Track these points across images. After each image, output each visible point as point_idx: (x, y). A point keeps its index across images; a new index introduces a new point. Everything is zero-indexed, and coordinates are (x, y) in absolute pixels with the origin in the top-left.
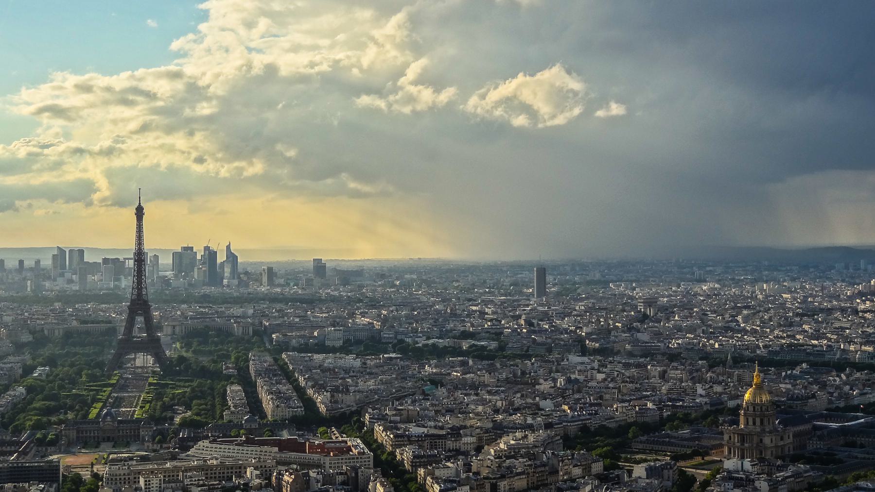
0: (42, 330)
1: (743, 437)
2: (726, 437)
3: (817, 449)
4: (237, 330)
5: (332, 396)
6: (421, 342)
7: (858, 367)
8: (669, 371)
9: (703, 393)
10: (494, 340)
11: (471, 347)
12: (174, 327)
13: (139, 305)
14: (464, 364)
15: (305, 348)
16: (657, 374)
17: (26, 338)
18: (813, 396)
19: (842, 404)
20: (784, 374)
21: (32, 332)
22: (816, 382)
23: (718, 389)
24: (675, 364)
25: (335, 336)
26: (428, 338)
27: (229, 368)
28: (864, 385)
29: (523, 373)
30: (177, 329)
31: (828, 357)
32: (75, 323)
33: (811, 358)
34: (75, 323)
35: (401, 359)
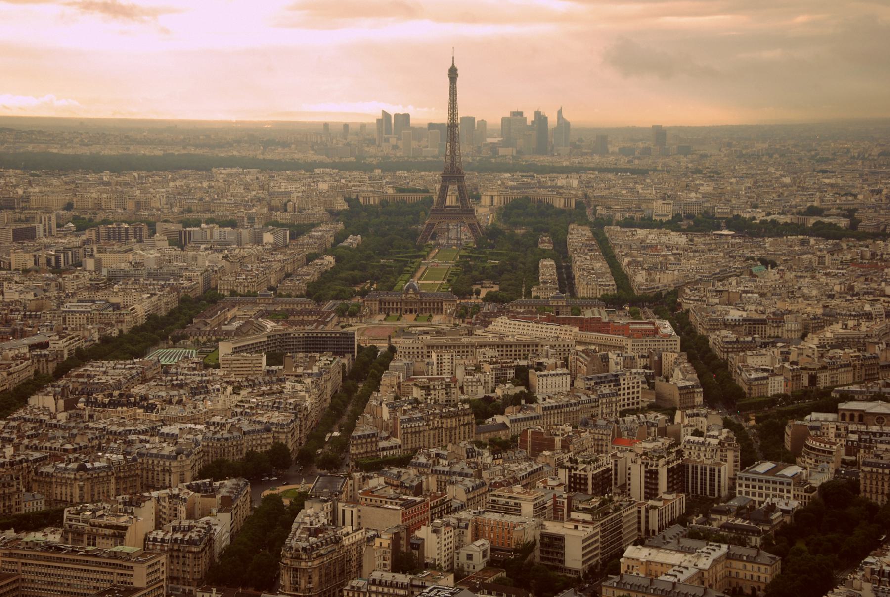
0: (357, 198)
4: (559, 203)
5: (650, 274)
6: (760, 216)
10: (844, 216)
11: (815, 224)
12: (492, 197)
13: (452, 174)
14: (803, 243)
15: (629, 224)
17: (341, 205)
21: (348, 200)
25: (662, 210)
26: (769, 214)
27: (546, 245)
29: (873, 255)
30: (496, 199)
32: (391, 191)
34: (391, 191)
35: (733, 236)
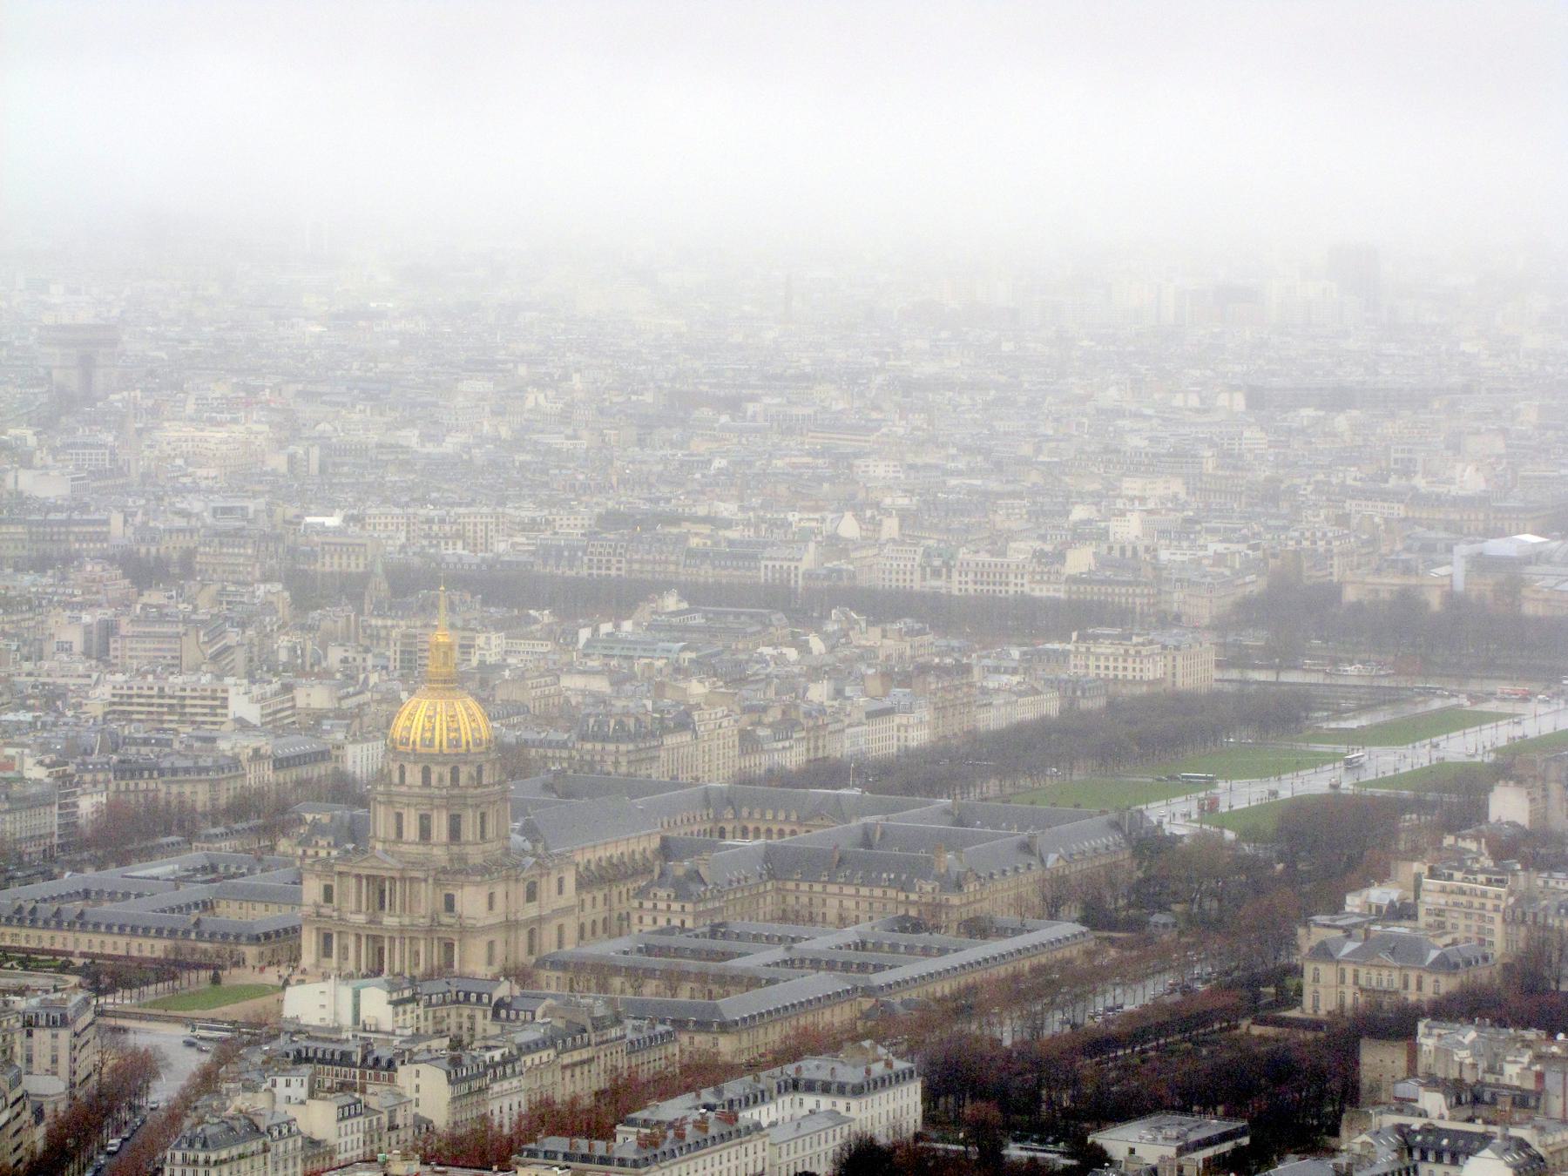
1: (379, 892)
2: (312, 890)
3: (669, 931)
7: (882, 606)
8: (125, 627)
9: (253, 714)
16: (75, 637)
18: (684, 723)
19: (793, 756)
20: (584, 634)
22: (704, 667)
23: (314, 696)
24: (154, 597)
28: (888, 677)
31: (764, 572)
33: (706, 573)
